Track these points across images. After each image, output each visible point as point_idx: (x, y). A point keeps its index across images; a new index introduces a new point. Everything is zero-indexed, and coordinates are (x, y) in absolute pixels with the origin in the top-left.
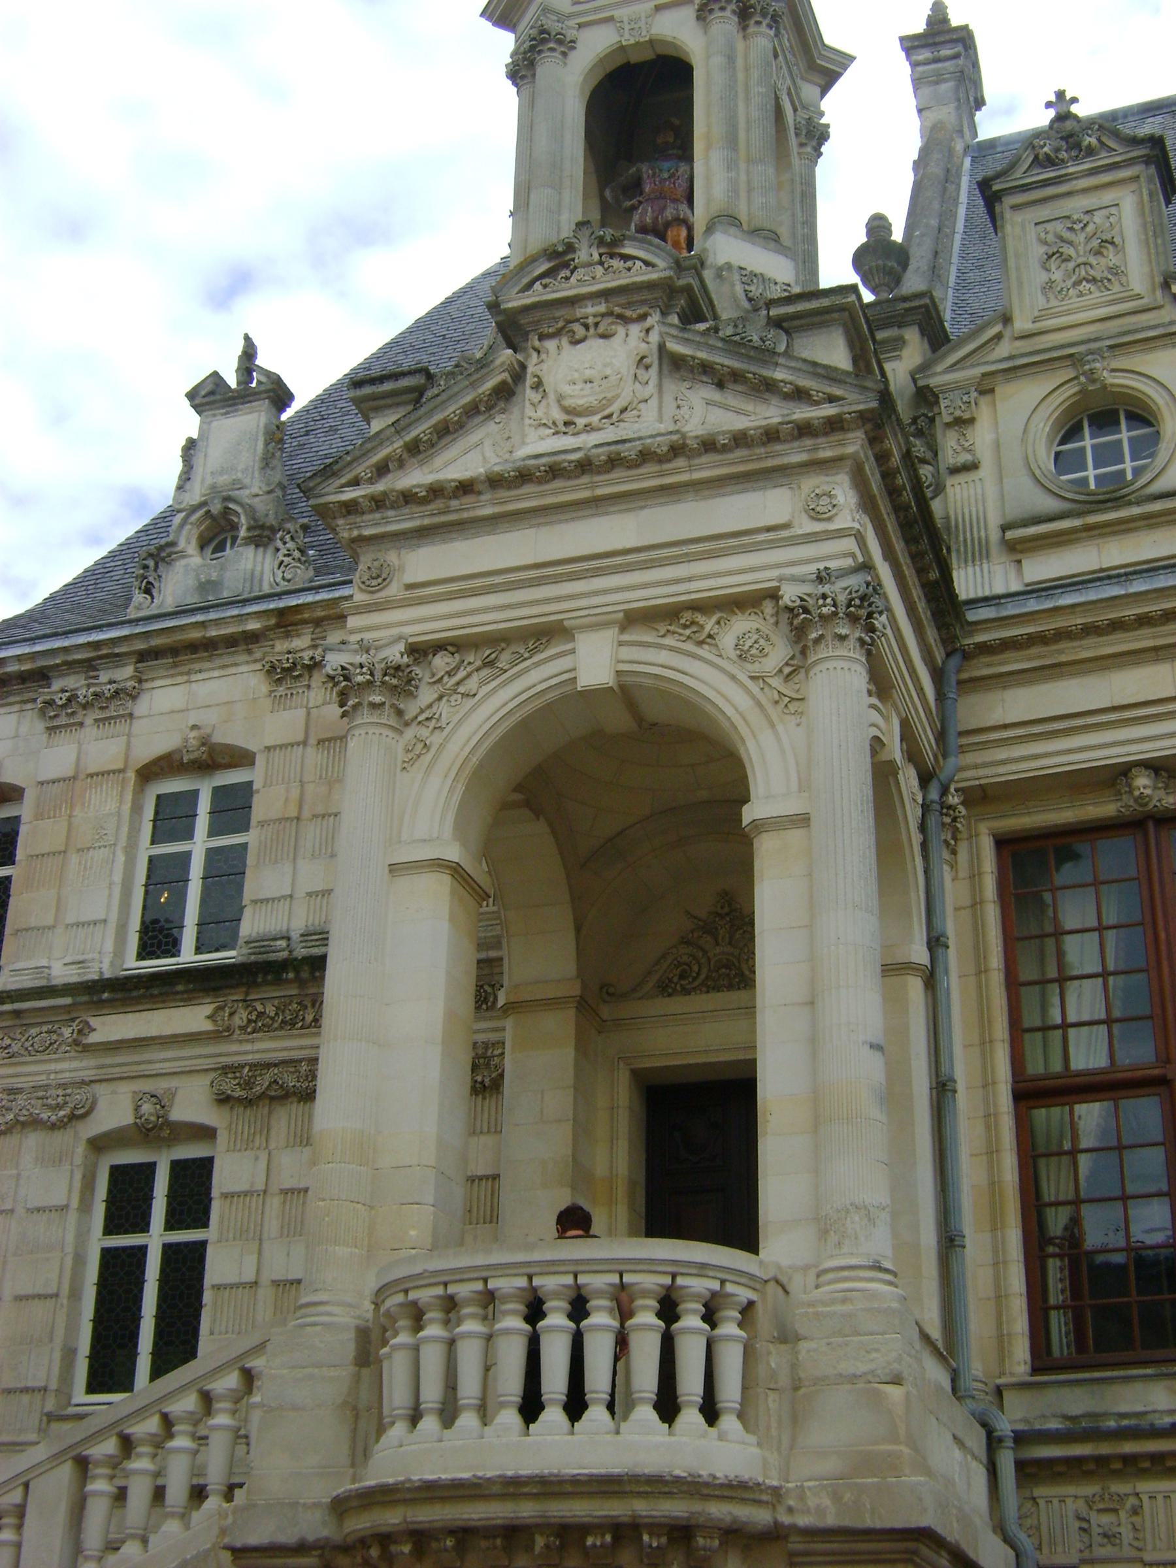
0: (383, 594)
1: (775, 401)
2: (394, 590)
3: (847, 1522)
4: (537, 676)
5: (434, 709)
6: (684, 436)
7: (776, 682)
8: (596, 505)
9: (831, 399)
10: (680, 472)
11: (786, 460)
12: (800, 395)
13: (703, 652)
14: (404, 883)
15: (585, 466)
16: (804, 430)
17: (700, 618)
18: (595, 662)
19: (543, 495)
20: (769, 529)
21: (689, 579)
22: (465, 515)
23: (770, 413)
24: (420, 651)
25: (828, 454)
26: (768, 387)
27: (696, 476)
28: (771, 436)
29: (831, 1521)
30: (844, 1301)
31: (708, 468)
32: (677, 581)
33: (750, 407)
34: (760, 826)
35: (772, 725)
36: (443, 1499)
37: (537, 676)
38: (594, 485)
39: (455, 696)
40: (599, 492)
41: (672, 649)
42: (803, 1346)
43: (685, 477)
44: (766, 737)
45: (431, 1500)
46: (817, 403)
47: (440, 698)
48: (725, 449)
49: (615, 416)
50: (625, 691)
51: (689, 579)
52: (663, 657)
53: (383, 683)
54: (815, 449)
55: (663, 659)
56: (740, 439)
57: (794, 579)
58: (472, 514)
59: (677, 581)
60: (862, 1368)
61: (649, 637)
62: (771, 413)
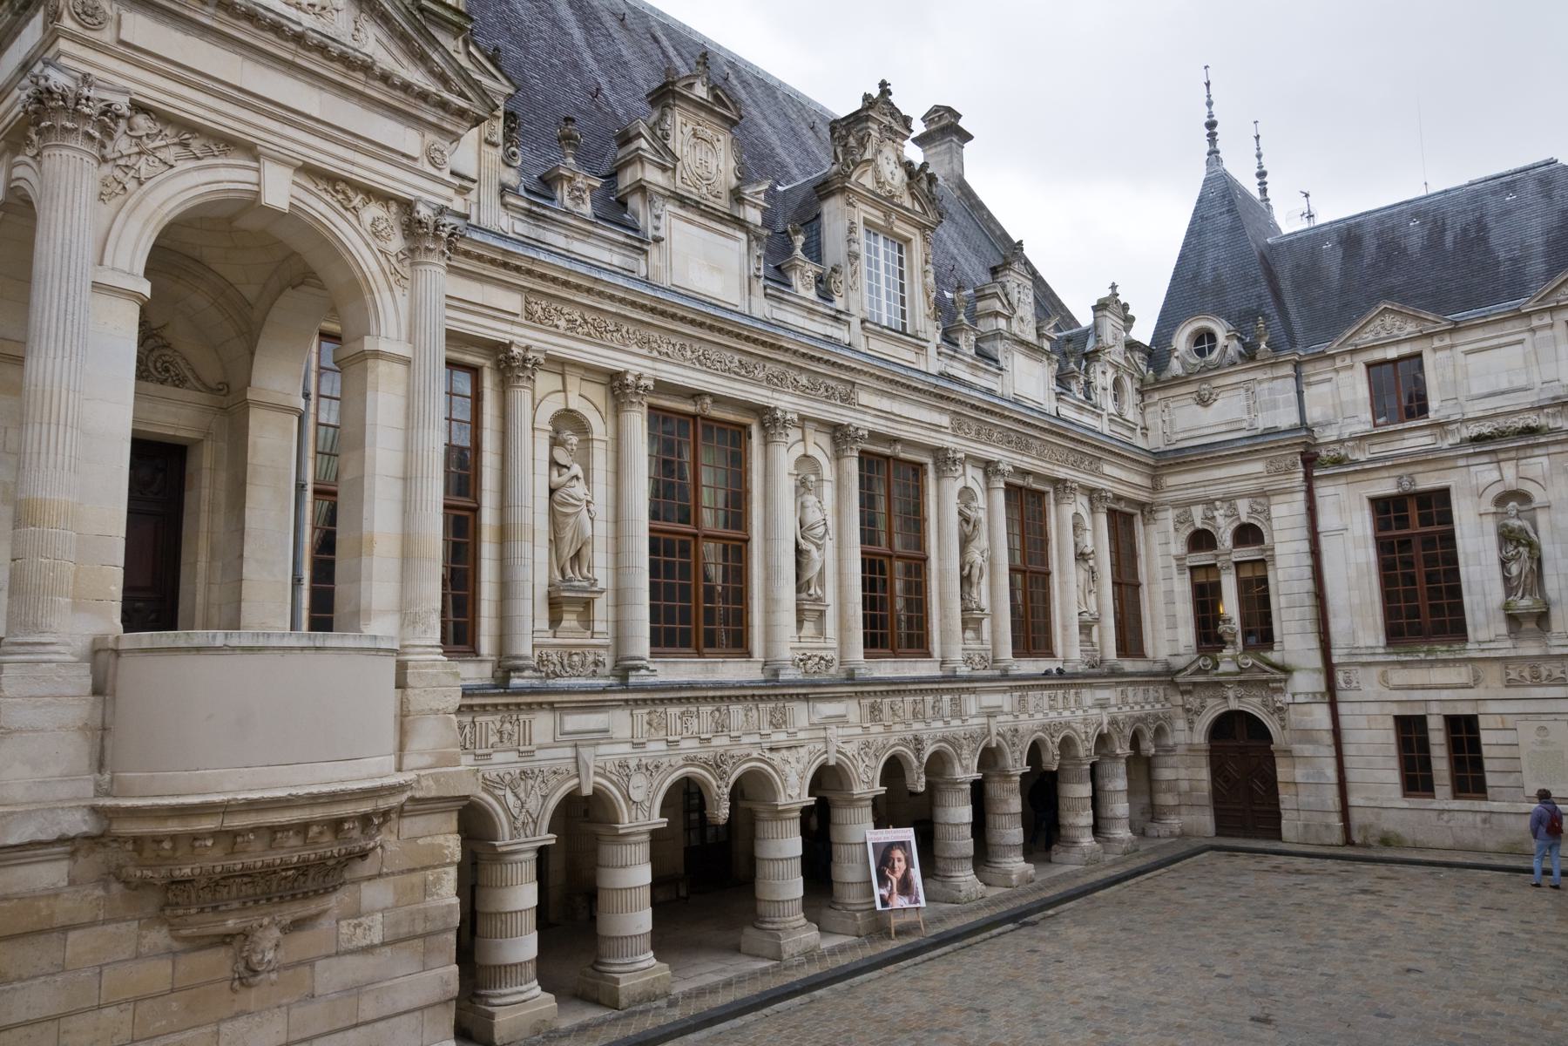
0: (88, 33)
1: (422, 69)
2: (106, 36)
3: (441, 794)
4: (229, 175)
5: (134, 159)
6: (374, 63)
7: (393, 260)
8: (292, 67)
9: (462, 95)
10: (357, 81)
11: (423, 115)
12: (443, 79)
13: (349, 215)
14: (104, 301)
15: (299, 39)
16: (444, 105)
17: (350, 193)
18: (279, 189)
19: (255, 36)
20: (404, 155)
21: (353, 164)
22: (187, 13)
23: (417, 77)
24: (138, 108)
25: (449, 127)
26: (422, 59)
27: (368, 91)
28: (424, 96)
29: (433, 794)
30: (433, 666)
31: (376, 91)
32: (345, 160)
33: (405, 62)
34: (377, 354)
35: (391, 289)
36: (257, 810)
37: (229, 175)
38: (296, 54)
39: (151, 158)
40: (298, 61)
41: (327, 203)
42: (409, 691)
43: (360, 88)
44: (387, 295)
45: (248, 811)
46: (450, 91)
47: (140, 153)
48: (394, 86)
49: (317, 9)
50: (293, 217)
51: (353, 164)
52: (322, 207)
53: (75, 110)
54: (442, 119)
55: (320, 206)
56: (406, 87)
57: (428, 204)
58: (192, 15)
59: (345, 160)
60: (442, 706)
61: (311, 186)
62: (417, 77)
